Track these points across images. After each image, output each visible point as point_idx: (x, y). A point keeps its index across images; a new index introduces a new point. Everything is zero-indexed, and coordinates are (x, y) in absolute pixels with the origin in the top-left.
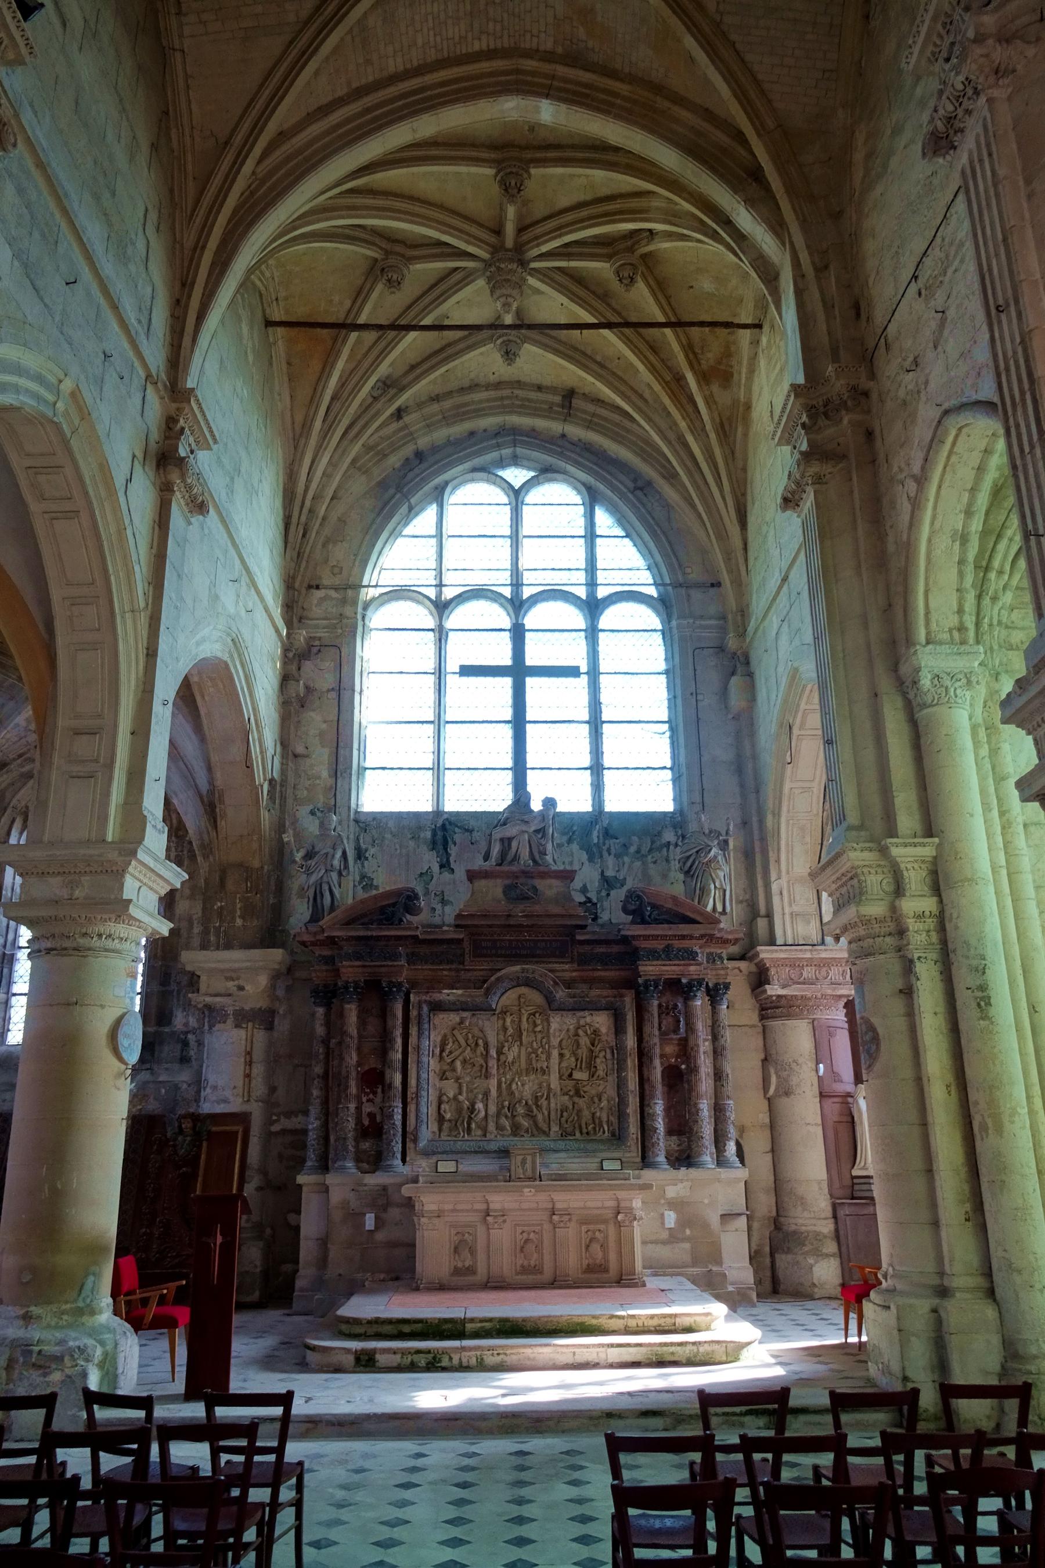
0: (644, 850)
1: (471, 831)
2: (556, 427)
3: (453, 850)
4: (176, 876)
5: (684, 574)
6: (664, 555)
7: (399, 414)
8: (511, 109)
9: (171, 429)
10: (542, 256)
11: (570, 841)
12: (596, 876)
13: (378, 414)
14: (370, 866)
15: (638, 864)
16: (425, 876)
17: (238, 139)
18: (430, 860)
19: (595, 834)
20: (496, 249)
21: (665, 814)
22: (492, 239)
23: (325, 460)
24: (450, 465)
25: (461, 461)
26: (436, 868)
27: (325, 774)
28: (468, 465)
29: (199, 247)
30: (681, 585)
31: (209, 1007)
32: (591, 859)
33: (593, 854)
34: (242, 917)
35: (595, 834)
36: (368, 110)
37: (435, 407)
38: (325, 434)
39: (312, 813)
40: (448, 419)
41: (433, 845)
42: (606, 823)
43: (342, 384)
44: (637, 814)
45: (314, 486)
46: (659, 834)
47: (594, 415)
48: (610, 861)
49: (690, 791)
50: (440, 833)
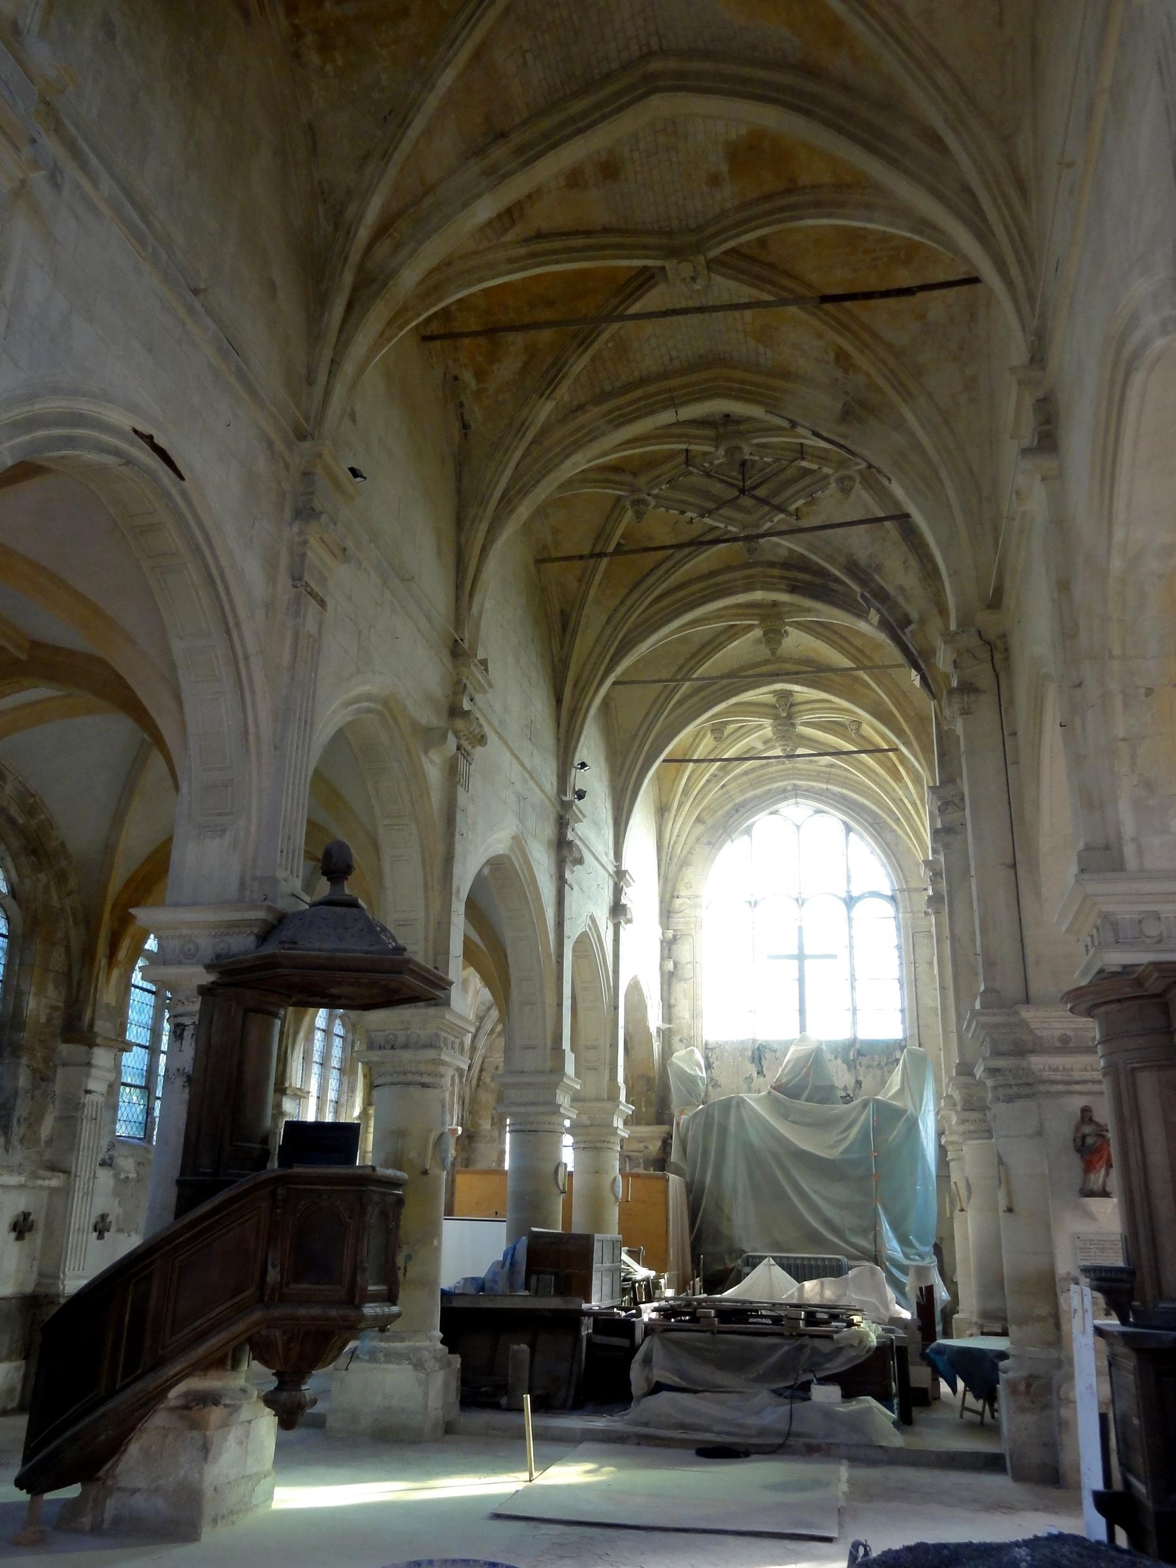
0: (883, 1063)
1: (775, 1051)
2: (825, 786)
3: (765, 1064)
4: (629, 1109)
5: (907, 881)
6: (894, 870)
7: (723, 786)
8: (778, 686)
9: (618, 891)
10: (803, 724)
11: (836, 1058)
12: (853, 1081)
13: (710, 791)
14: (715, 1073)
15: (879, 1072)
16: (749, 1079)
17: (641, 734)
18: (752, 1070)
19: (852, 1053)
20: (776, 717)
21: (896, 1041)
22: (774, 712)
23: (680, 822)
24: (757, 812)
25: (763, 809)
26: (755, 1075)
27: (687, 1016)
28: (768, 811)
29: (623, 790)
30: (904, 890)
31: (628, 1157)
32: (849, 1070)
33: (851, 1065)
34: (646, 1106)
35: (852, 1053)
36: (704, 698)
37: (745, 779)
38: (681, 804)
39: (681, 1040)
40: (753, 785)
41: (753, 1060)
42: (858, 1046)
43: (689, 778)
44: (877, 1041)
45: (674, 838)
46: (891, 1054)
47: (846, 778)
48: (861, 1070)
49: (911, 1026)
50: (756, 1055)
